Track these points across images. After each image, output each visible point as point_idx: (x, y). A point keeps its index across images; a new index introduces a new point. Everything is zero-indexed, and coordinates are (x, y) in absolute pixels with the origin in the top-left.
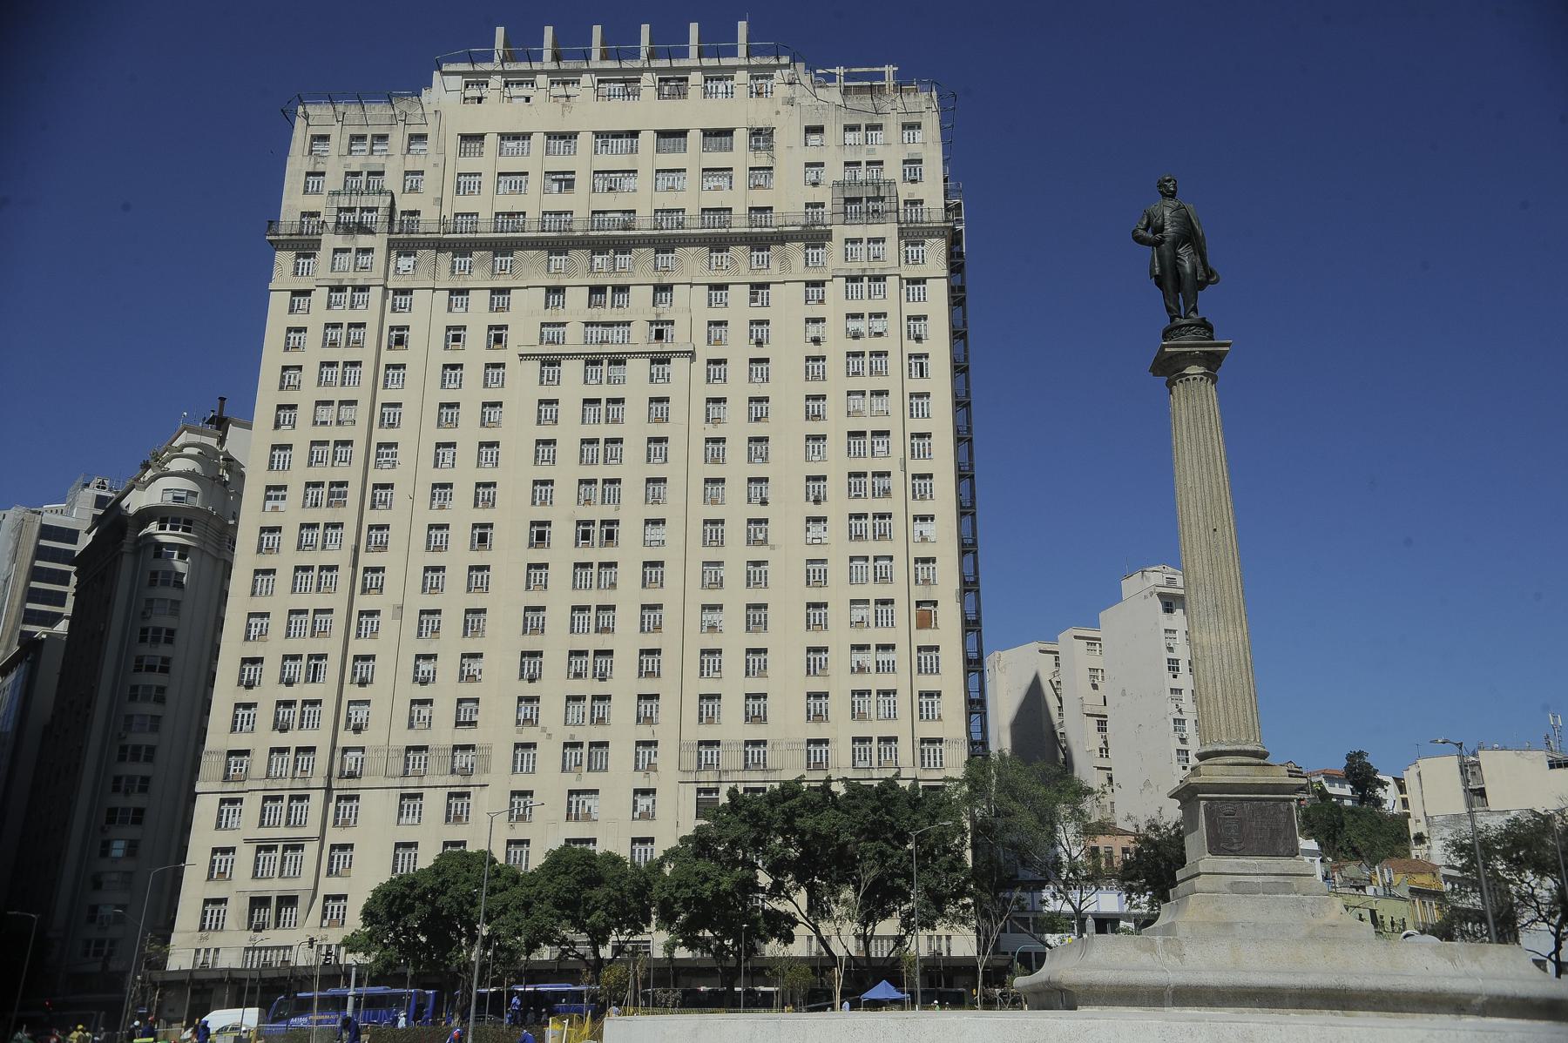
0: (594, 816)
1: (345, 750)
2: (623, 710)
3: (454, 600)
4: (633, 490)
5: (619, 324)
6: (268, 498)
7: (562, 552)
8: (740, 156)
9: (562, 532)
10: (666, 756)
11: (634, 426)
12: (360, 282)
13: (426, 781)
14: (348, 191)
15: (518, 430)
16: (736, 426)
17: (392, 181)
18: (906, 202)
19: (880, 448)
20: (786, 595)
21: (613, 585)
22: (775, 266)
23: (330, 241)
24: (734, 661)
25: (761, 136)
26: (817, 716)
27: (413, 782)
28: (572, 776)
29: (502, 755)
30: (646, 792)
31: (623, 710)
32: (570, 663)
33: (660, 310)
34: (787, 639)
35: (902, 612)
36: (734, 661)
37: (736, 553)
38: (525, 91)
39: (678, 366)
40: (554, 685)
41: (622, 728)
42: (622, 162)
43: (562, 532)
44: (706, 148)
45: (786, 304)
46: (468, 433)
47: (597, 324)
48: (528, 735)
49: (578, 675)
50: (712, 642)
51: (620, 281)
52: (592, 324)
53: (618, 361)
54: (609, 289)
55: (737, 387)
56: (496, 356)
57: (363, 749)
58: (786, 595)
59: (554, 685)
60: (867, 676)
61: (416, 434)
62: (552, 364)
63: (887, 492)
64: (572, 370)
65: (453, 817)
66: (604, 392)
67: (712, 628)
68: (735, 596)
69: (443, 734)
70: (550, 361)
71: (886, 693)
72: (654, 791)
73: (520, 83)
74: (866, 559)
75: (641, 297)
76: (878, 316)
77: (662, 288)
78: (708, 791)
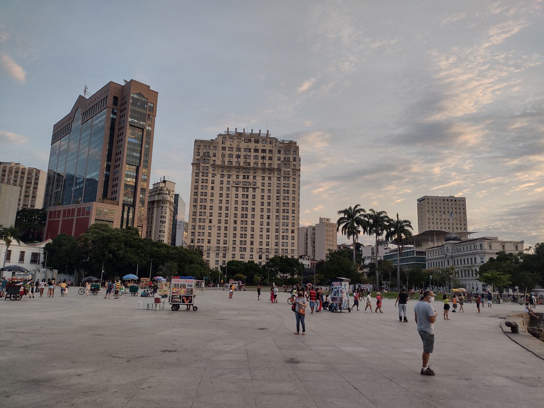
4: (250, 210)
7: (239, 219)
8: (267, 155)
9: (239, 215)
10: (255, 250)
11: (250, 199)
16: (266, 201)
25: (271, 151)
29: (231, 249)
35: (290, 231)
36: (264, 237)
40: (238, 239)
41: (248, 246)
42: (249, 154)
43: (239, 215)
44: (262, 152)
46: (224, 199)
48: (234, 246)
50: (261, 233)
53: (248, 188)
55: (266, 194)
56: (228, 186)
58: (273, 227)
59: (238, 239)
61: (216, 198)
63: (288, 212)
64: (240, 189)
66: (246, 193)
67: (261, 231)
68: (265, 227)
69: (222, 245)
70: (237, 188)
75: (251, 178)
77: (255, 177)
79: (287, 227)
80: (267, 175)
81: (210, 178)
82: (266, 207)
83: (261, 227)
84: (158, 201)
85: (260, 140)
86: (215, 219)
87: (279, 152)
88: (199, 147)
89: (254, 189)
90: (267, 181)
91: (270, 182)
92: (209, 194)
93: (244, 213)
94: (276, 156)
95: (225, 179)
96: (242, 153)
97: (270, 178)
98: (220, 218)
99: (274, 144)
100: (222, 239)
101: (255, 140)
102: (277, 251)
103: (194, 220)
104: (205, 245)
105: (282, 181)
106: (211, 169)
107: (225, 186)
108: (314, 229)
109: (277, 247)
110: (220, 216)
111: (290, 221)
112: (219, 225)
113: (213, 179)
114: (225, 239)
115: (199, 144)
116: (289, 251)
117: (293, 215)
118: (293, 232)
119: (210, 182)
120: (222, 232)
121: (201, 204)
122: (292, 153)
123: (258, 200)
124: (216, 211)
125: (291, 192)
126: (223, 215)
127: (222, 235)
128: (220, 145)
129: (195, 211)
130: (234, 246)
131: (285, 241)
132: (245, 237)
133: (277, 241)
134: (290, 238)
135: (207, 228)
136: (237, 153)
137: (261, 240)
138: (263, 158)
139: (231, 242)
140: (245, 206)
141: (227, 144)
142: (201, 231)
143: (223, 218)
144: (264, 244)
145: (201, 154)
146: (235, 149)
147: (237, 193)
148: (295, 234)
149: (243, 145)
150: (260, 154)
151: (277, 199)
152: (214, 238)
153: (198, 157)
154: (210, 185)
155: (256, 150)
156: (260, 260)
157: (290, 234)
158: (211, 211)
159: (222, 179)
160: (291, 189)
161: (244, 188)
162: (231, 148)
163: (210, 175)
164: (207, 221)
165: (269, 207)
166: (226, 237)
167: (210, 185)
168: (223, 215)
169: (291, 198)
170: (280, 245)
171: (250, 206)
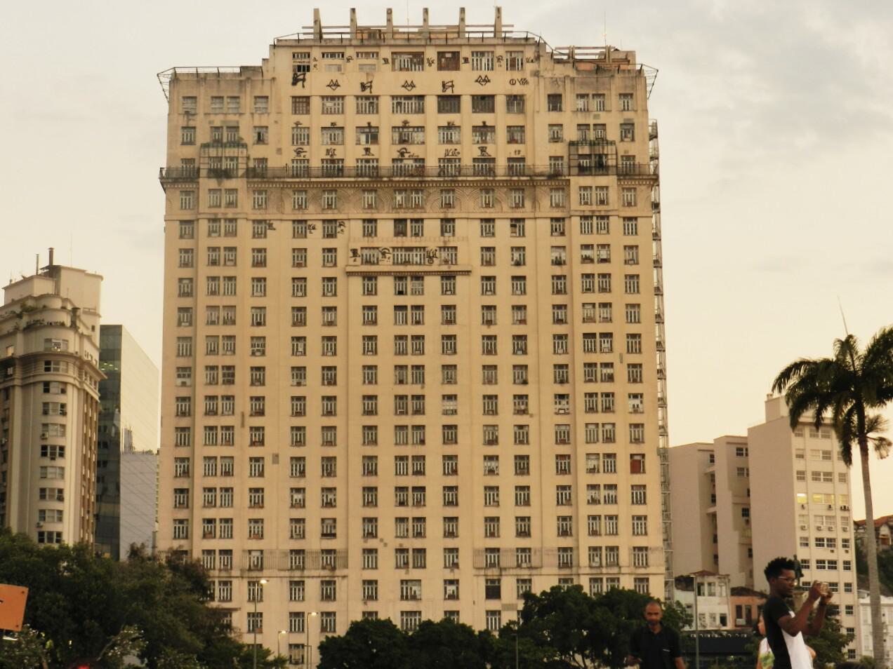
0: (418, 597)
1: (250, 552)
2: (434, 528)
3: (313, 452)
4: (433, 376)
5: (416, 248)
6: (179, 376)
7: (386, 420)
8: (501, 118)
9: (386, 404)
10: (465, 559)
11: (432, 328)
12: (230, 216)
13: (306, 573)
14: (217, 143)
15: (352, 329)
17: (247, 134)
18: (622, 157)
19: (606, 345)
20: (543, 450)
21: (423, 442)
22: (528, 204)
23: (207, 183)
24: (507, 495)
25: (516, 102)
26: (564, 533)
27: (298, 573)
28: (403, 571)
29: (356, 558)
30: (451, 582)
31: (434, 528)
32: (396, 495)
33: (446, 239)
34: (544, 480)
35: (623, 463)
36: (507, 495)
37: (507, 420)
38: (337, 61)
39: (460, 280)
40: (387, 511)
41: (434, 541)
42: (415, 120)
43: (386, 404)
45: (538, 233)
47: (401, 248)
48: (372, 543)
49: (402, 504)
50: (492, 481)
51: (416, 216)
52: (397, 248)
53: (418, 277)
54: (409, 222)
55: (504, 298)
56: (329, 273)
57: (262, 552)
58: (543, 450)
59: (387, 511)
60: (598, 507)
62: (370, 279)
63: (611, 378)
65: (328, 596)
67: (491, 472)
68: (507, 450)
69: (313, 542)
70: (370, 277)
71: (611, 518)
72: (457, 581)
73: (333, 55)
74: (597, 425)
75: (432, 227)
76: (603, 246)
78: (493, 581)
79: (609, 448)
80: (503, 212)
81: (245, 241)
82: (505, 358)
83: (491, 450)
84: (28, 361)
85: (465, 52)
86: (277, 424)
87: (555, 101)
88: (189, 105)
89: (448, 277)
90: (503, 237)
91: (518, 242)
92: (244, 316)
93: (410, 389)
94: (539, 119)
95: (315, 242)
96: (387, 119)
97: (517, 223)
98: (298, 422)
99: (529, 67)
100: (314, 514)
101: (441, 55)
102: (566, 558)
103: (184, 435)
104: (239, 542)
105: (576, 235)
106: (246, 202)
107: (315, 271)
108: (741, 448)
109: (566, 542)
110: (300, 413)
111: (621, 418)
112: (298, 452)
113: (259, 243)
114: (329, 513)
115: (187, 89)
116: (625, 557)
117: (636, 388)
118: (637, 465)
119: (245, 257)
120: (314, 482)
121: (212, 360)
122: (614, 102)
123: (469, 329)
124: (279, 390)
125: (618, 283)
126: (314, 406)
127: (314, 497)
128: (286, 90)
129: (184, 393)
130: (372, 543)
131: (603, 510)
132: (419, 503)
133: (565, 511)
134: (624, 494)
135: (242, 466)
136: (363, 120)
137: (492, 512)
138: (483, 130)
139: (357, 528)
140: (410, 360)
141: (316, 84)
142: (219, 482)
143: (314, 421)
144: (508, 528)
145: (203, 136)
146: (351, 104)
147: (370, 301)
148: (651, 477)
149: (388, 82)
150: (467, 118)
151: (559, 321)
152: (277, 513)
153: (189, 152)
154: (245, 271)
155: (449, 102)
156: (494, 605)
157: (624, 478)
158: (258, 391)
159: (300, 243)
160: (617, 270)
161: (400, 277)
162: (334, 100)
163: (245, 228)
164: (243, 436)
165: (520, 360)
166: (329, 504)
167: (245, 271)
168: (314, 406)
169: (619, 312)
170: (582, 527)
171: (432, 359)
